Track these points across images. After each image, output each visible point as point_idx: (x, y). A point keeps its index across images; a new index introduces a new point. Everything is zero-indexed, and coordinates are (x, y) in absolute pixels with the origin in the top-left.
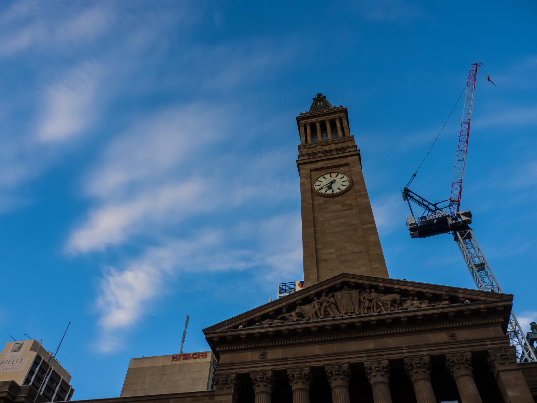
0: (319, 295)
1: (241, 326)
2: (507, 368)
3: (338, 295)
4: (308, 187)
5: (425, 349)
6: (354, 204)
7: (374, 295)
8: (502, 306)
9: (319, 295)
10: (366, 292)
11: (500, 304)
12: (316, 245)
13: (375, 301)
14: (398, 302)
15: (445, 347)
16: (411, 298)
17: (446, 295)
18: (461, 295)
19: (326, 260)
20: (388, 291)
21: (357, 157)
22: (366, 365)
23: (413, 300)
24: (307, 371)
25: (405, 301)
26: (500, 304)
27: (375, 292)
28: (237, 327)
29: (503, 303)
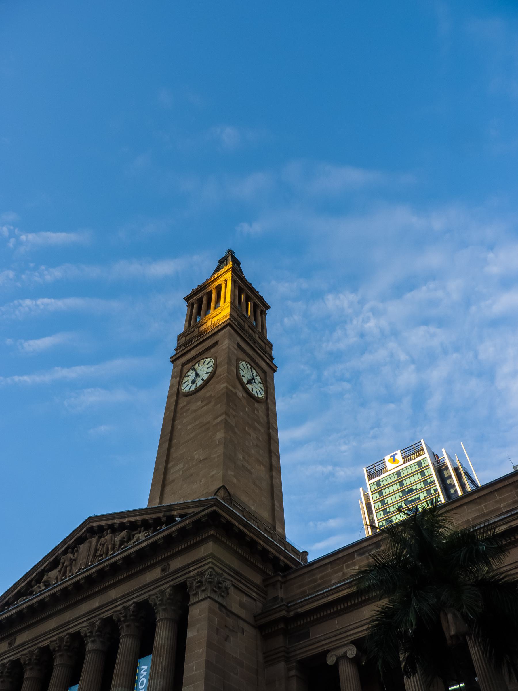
0: (65, 552)
2: (200, 598)
4: (175, 389)
5: (135, 595)
8: (205, 515)
9: (65, 552)
11: (203, 513)
15: (152, 587)
17: (163, 517)
18: (175, 513)
21: (228, 328)
23: (140, 532)
25: (134, 535)
26: (203, 513)
27: (111, 533)
29: (206, 512)
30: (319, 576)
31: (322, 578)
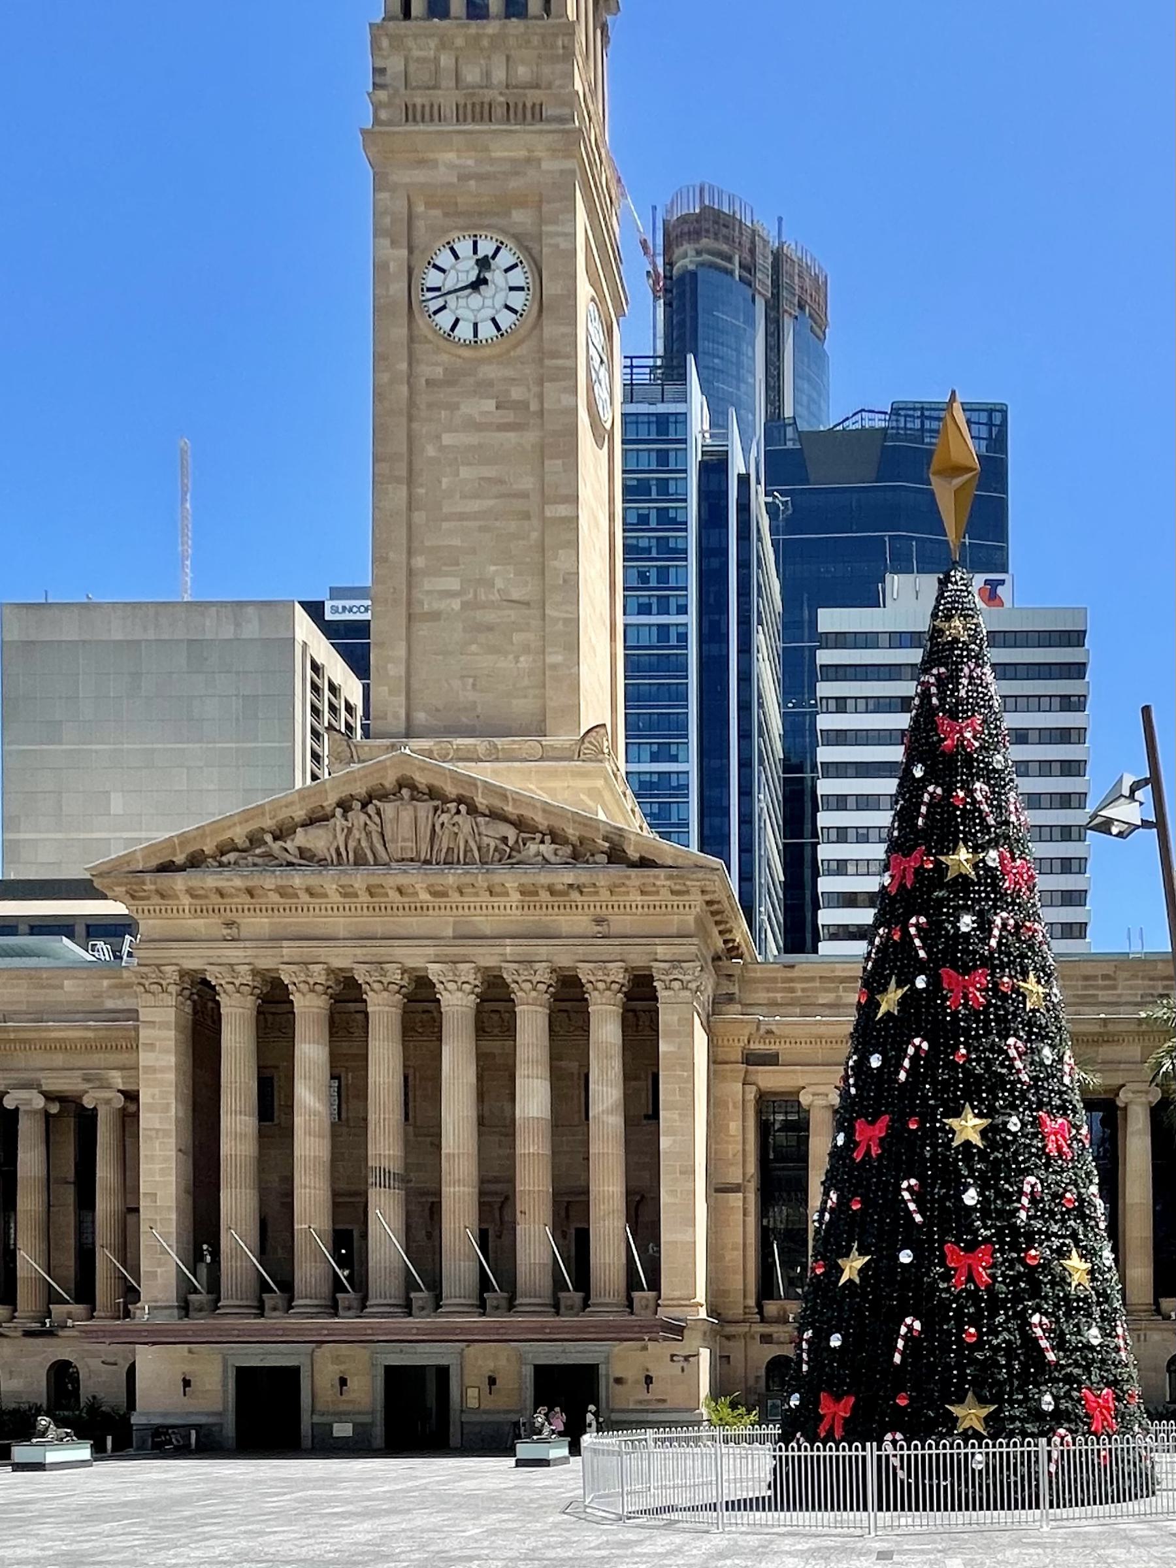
3: (388, 809)
9: (344, 805)
10: (448, 811)
13: (461, 837)
14: (511, 843)
16: (539, 836)
20: (496, 815)
23: (542, 842)
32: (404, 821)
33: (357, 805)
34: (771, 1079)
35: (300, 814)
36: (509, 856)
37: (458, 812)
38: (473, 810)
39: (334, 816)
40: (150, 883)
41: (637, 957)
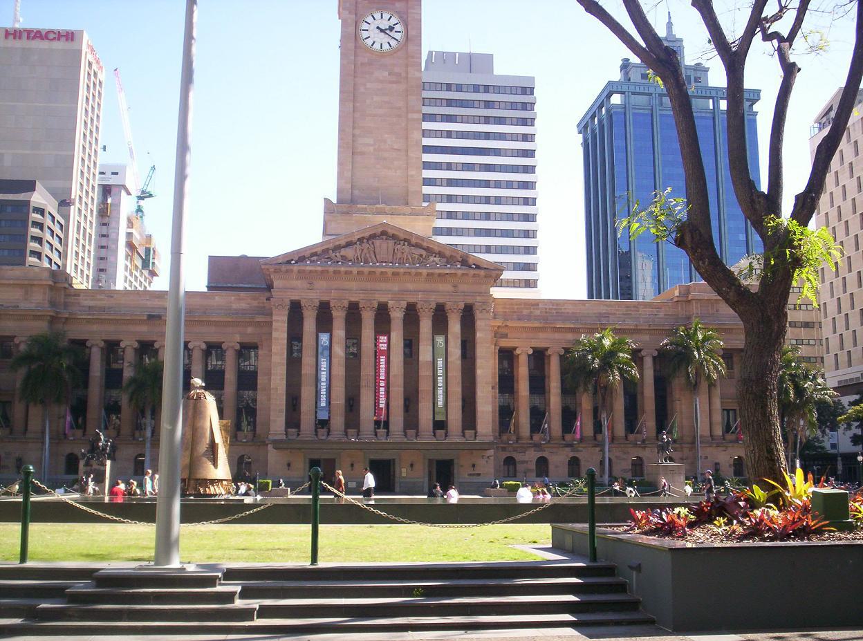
1: (293, 262)
3: (377, 242)
6: (403, 75)
7: (406, 248)
9: (361, 240)
10: (400, 244)
12: (354, 128)
13: (405, 254)
14: (424, 256)
18: (471, 262)
19: (362, 153)
20: (418, 246)
22: (391, 303)
23: (435, 257)
24: (346, 304)
28: (289, 262)
30: (516, 307)
31: (517, 308)
32: (383, 246)
33: (365, 241)
34: (505, 343)
35: (343, 243)
36: (422, 260)
37: (404, 245)
38: (410, 244)
39: (356, 243)
40: (284, 268)
41: (469, 301)
